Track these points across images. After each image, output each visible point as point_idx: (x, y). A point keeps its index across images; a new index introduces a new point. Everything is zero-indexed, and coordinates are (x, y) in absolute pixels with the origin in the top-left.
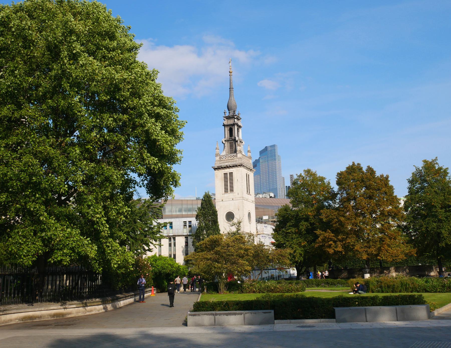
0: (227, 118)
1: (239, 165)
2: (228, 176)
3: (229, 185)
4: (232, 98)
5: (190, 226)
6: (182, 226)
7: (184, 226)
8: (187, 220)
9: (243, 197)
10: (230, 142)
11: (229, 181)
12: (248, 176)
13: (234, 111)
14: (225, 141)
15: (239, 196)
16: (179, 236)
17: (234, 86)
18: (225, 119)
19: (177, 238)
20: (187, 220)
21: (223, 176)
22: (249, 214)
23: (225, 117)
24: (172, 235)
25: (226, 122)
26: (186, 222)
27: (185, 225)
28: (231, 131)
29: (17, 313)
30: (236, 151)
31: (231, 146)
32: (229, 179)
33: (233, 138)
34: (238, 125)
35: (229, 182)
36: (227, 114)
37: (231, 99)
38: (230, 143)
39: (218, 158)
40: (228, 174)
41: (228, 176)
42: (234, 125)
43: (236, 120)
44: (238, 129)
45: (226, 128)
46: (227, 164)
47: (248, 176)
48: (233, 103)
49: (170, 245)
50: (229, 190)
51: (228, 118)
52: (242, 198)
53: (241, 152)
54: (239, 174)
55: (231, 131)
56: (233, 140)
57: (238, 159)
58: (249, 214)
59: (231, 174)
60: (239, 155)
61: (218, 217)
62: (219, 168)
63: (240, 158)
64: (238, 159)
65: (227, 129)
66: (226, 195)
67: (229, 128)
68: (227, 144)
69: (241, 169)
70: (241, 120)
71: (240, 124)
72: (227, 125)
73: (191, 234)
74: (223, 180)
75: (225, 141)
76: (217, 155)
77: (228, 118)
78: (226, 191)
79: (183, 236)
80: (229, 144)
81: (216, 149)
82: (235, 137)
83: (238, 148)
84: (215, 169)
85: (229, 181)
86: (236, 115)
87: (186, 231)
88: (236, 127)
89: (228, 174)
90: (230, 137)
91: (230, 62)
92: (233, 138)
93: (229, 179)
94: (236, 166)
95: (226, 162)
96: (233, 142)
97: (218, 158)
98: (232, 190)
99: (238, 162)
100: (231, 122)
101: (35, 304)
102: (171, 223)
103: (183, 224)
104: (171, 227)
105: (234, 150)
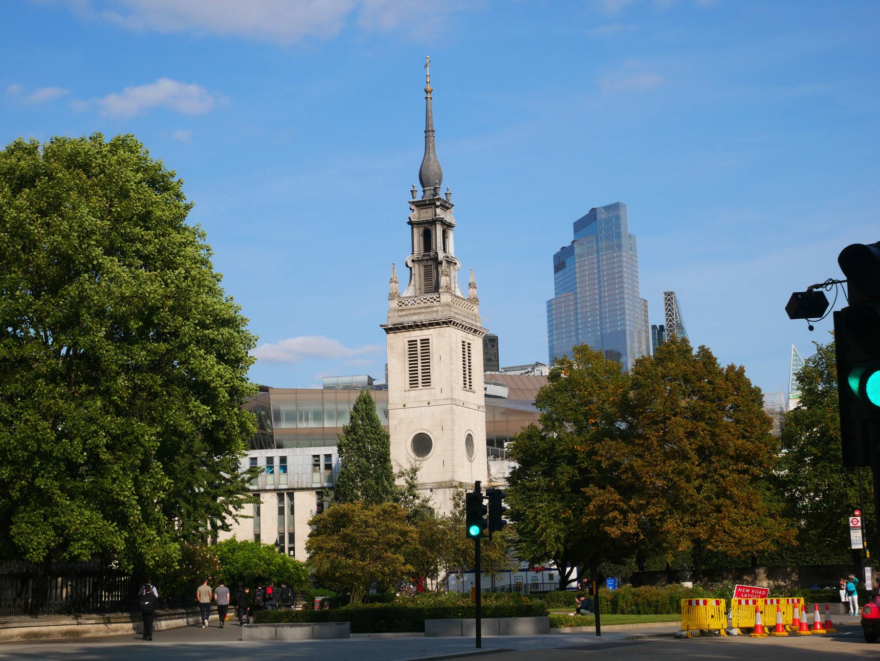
0: (417, 206)
2: (419, 348)
3: (420, 369)
4: (432, 155)
5: (328, 467)
6: (310, 468)
7: (315, 465)
8: (322, 451)
9: (452, 399)
11: (419, 358)
12: (466, 347)
13: (435, 189)
14: (413, 261)
15: (444, 396)
16: (302, 489)
17: (436, 126)
18: (413, 207)
19: (297, 494)
20: (322, 451)
21: (407, 346)
22: (469, 440)
23: (413, 203)
24: (285, 487)
25: (415, 216)
26: (318, 456)
27: (316, 465)
28: (427, 238)
29: (18, 629)
30: (436, 288)
31: (427, 275)
32: (419, 355)
33: (432, 254)
34: (443, 223)
35: (419, 362)
36: (419, 197)
37: (429, 159)
39: (394, 304)
40: (419, 343)
41: (419, 348)
42: (433, 222)
43: (438, 211)
44: (444, 232)
45: (415, 229)
46: (415, 318)
47: (466, 347)
48: (433, 167)
49: (281, 511)
50: (420, 381)
51: (420, 205)
52: (449, 402)
53: (448, 288)
54: (445, 344)
55: (427, 238)
56: (431, 259)
57: (443, 306)
58: (469, 440)
59: (425, 342)
60: (445, 298)
61: (391, 448)
62: (397, 329)
63: (448, 305)
64: (443, 306)
66: (413, 393)
67: (421, 230)
68: (417, 270)
69: (450, 330)
70: (453, 210)
71: (448, 217)
73: (330, 485)
75: (413, 261)
76: (392, 297)
77: (420, 205)
78: (413, 383)
79: (312, 489)
80: (422, 269)
81: (391, 281)
82: (437, 253)
83: (443, 280)
84: (388, 330)
85: (419, 358)
86: (439, 199)
87: (319, 479)
88: (439, 229)
89: (419, 343)
90: (425, 251)
91: (426, 66)
93: (419, 355)
94: (438, 324)
95: (414, 314)
96: (430, 266)
97: (394, 304)
98: (427, 382)
99: (440, 316)
100: (426, 215)
101: (40, 617)
102: (283, 460)
103: (310, 461)
104: (284, 468)
105: (432, 286)
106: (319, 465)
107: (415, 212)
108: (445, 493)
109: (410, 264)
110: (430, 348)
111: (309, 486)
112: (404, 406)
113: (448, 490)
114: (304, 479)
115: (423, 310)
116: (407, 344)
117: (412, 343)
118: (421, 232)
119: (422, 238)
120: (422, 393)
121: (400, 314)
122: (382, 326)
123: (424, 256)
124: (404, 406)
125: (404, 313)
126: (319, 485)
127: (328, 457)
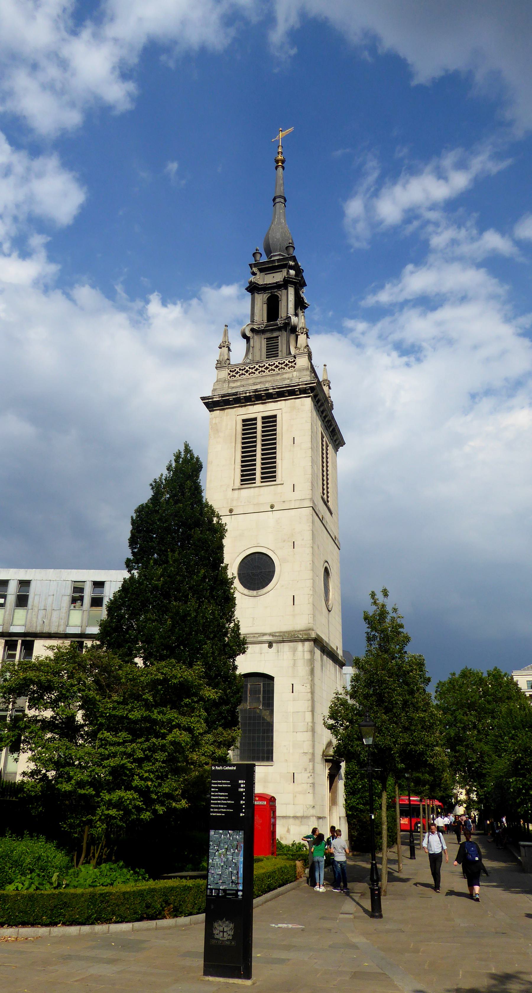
1: (303, 391)
3: (259, 458)
6: (67, 600)
8: (89, 576)
10: (268, 335)
14: (253, 330)
15: (298, 494)
18: (255, 270)
21: (240, 427)
23: (256, 265)
24: (21, 630)
27: (77, 597)
33: (280, 322)
38: (268, 339)
39: (224, 373)
51: (266, 268)
57: (300, 370)
59: (270, 421)
66: (248, 493)
72: (263, 289)
74: (239, 441)
75: (253, 330)
78: (247, 477)
80: (264, 342)
90: (269, 320)
92: (280, 322)
95: (254, 384)
98: (269, 474)
103: (69, 591)
104: (22, 601)
106: (81, 599)
107: (258, 277)
108: (295, 650)
109: (248, 334)
110: (278, 428)
111: (61, 630)
113: (300, 645)
114: (55, 619)
115: (269, 379)
117: (248, 424)
118: (265, 299)
119: (265, 306)
120: (261, 493)
121: (232, 385)
122: (203, 399)
123: (266, 326)
124: (231, 511)
125: (239, 384)
126: (77, 631)
127: (99, 585)
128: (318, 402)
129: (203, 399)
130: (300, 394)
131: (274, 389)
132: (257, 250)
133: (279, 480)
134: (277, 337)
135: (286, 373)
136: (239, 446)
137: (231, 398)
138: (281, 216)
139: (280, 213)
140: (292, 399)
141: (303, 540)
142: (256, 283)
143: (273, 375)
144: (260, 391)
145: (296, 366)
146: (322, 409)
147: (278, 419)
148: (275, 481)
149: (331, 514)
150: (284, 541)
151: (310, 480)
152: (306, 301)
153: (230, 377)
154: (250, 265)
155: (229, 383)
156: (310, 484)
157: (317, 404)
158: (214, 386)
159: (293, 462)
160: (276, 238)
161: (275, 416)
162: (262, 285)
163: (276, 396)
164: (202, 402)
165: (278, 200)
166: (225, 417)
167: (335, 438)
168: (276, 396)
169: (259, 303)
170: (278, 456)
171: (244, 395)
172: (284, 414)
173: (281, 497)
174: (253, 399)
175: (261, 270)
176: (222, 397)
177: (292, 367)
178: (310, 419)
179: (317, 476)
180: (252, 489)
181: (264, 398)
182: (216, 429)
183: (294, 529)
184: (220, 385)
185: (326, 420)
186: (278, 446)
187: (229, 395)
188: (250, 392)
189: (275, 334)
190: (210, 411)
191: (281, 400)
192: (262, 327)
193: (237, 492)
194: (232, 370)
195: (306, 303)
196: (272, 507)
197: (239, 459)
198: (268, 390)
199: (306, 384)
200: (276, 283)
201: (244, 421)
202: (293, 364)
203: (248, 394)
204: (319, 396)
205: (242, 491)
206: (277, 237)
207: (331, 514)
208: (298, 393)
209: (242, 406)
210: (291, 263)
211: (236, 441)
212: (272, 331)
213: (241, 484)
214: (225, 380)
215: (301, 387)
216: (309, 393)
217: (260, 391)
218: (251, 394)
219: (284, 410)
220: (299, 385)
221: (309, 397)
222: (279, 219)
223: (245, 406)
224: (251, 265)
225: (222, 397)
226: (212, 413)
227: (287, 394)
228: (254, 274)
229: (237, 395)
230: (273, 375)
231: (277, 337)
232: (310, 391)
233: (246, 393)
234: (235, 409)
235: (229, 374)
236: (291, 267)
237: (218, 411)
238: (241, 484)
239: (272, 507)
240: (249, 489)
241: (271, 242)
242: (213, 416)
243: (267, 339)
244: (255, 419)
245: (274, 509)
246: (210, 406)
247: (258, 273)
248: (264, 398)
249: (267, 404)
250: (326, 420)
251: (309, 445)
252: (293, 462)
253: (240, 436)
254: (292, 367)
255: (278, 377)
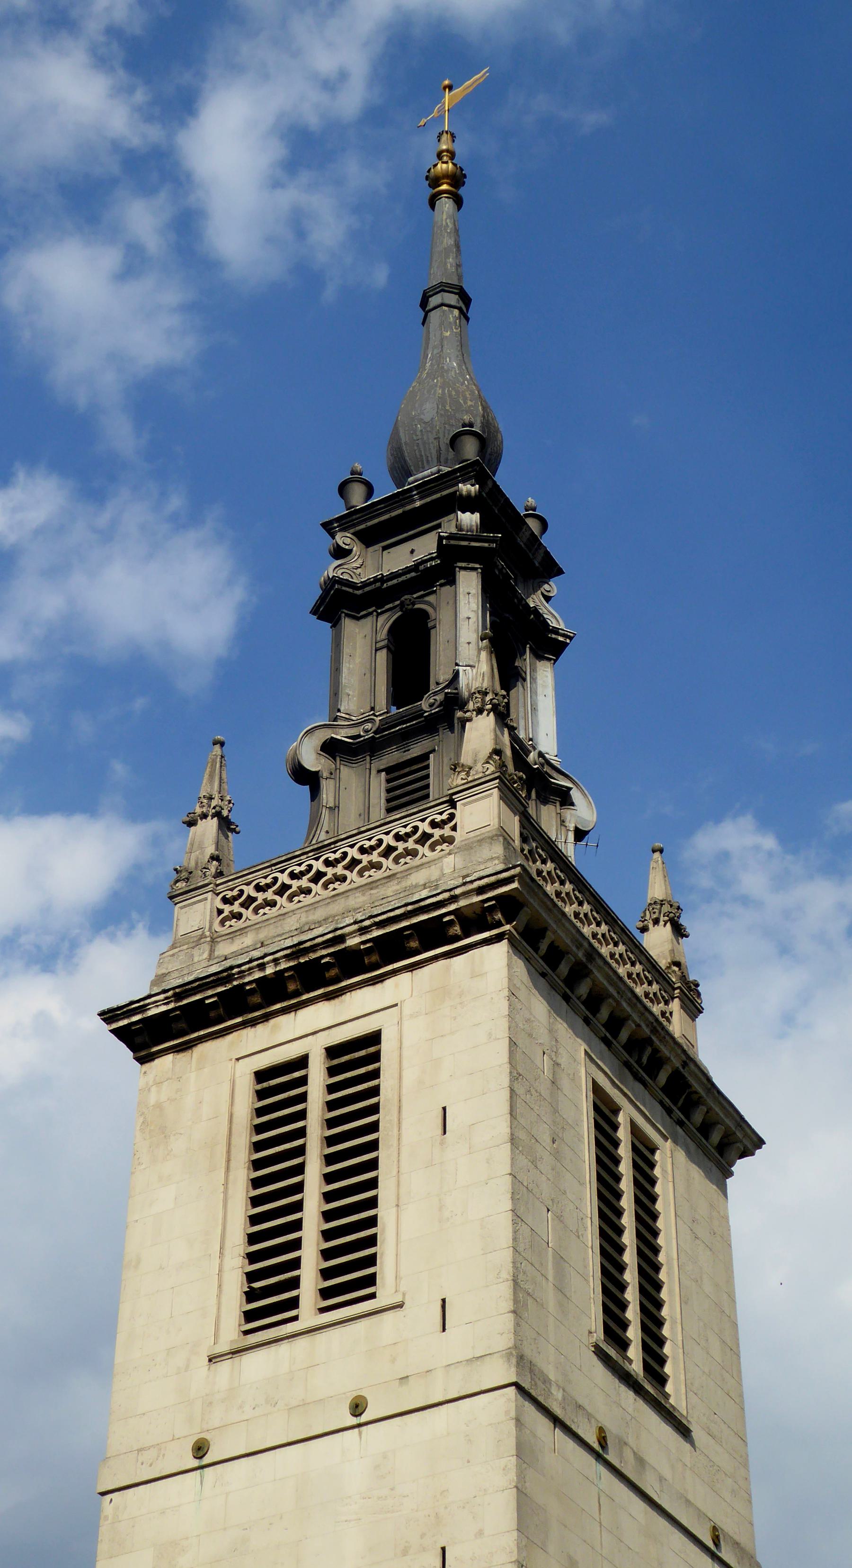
1: (474, 922)
10: (393, 756)
14: (330, 748)
15: (459, 1342)
23: (344, 523)
51: (379, 526)
57: (468, 847)
59: (357, 1057)
65: (362, 645)
67: (384, 622)
74: (243, 1155)
75: (330, 748)
78: (268, 1299)
80: (379, 785)
98: (352, 1275)
107: (354, 561)
109: (311, 760)
110: (386, 1082)
112: (200, 1449)
116: (246, 1087)
117: (278, 1085)
118: (383, 634)
119: (382, 655)
122: (109, 1016)
128: (554, 956)
129: (109, 1016)
130: (467, 936)
131: (363, 930)
132: (353, 473)
133: (385, 1293)
134: (425, 757)
135: (418, 867)
136: (242, 1175)
137: (209, 995)
138: (447, 350)
139: (442, 339)
140: (436, 958)
141: (480, 1533)
142: (341, 582)
143: (372, 885)
144: (313, 948)
145: (458, 836)
146: (583, 989)
147: (387, 1046)
148: (373, 1296)
149: (684, 1431)
150: (405, 1552)
151: (507, 1273)
152: (553, 624)
153: (222, 923)
154: (327, 526)
155: (213, 941)
156: (505, 1290)
157: (554, 968)
158: (160, 964)
159: (441, 1208)
160: (421, 421)
161: (374, 1038)
162: (365, 584)
163: (375, 958)
164: (106, 1027)
165: (434, 301)
166: (193, 1075)
167: (698, 1117)
168: (375, 958)
169: (359, 651)
170: (385, 1192)
171: (257, 975)
172: (406, 1024)
173: (393, 1360)
174: (291, 987)
175: (368, 538)
176: (178, 997)
177: (444, 840)
178: (504, 1024)
179: (560, 1259)
180: (284, 1346)
181: (333, 972)
182: (158, 1127)
183: (444, 1492)
184: (182, 956)
185: (624, 1035)
186: (383, 1154)
187: (202, 984)
188: (276, 961)
189: (416, 750)
190: (142, 1060)
191: (395, 972)
192: (366, 731)
193: (225, 1366)
194: (229, 894)
195: (556, 631)
196: (357, 1408)
197: (238, 1228)
198: (341, 939)
199: (481, 890)
200: (415, 568)
201: (261, 1076)
202: (447, 831)
203: (270, 970)
204: (549, 937)
205: (248, 1359)
206: (427, 418)
207: (684, 1431)
208: (457, 929)
209: (253, 1023)
210: (467, 488)
211: (228, 1161)
212: (405, 737)
213: (246, 1333)
214: (203, 936)
215: (462, 903)
216: (499, 924)
217: (313, 948)
218: (283, 965)
219: (407, 1010)
220: (454, 899)
221: (498, 938)
222: (439, 359)
223: (266, 1018)
224: (327, 526)
225: (178, 997)
226: (147, 1065)
227: (414, 944)
228: (340, 553)
229: (230, 979)
230: (372, 885)
231: (425, 757)
232: (499, 916)
233: (262, 967)
234: (230, 1038)
235: (220, 912)
236: (468, 504)
237: (170, 1058)
238: (246, 1333)
239: (357, 1408)
240: (273, 1348)
241: (404, 437)
242: (150, 1078)
243: (388, 770)
244: (302, 1062)
245: (364, 1418)
246: (138, 1040)
247: (357, 548)
248: (333, 972)
249: (347, 997)
250: (624, 1035)
251: (503, 1128)
252: (441, 1208)
253: (244, 1138)
254: (444, 840)
255: (391, 889)
